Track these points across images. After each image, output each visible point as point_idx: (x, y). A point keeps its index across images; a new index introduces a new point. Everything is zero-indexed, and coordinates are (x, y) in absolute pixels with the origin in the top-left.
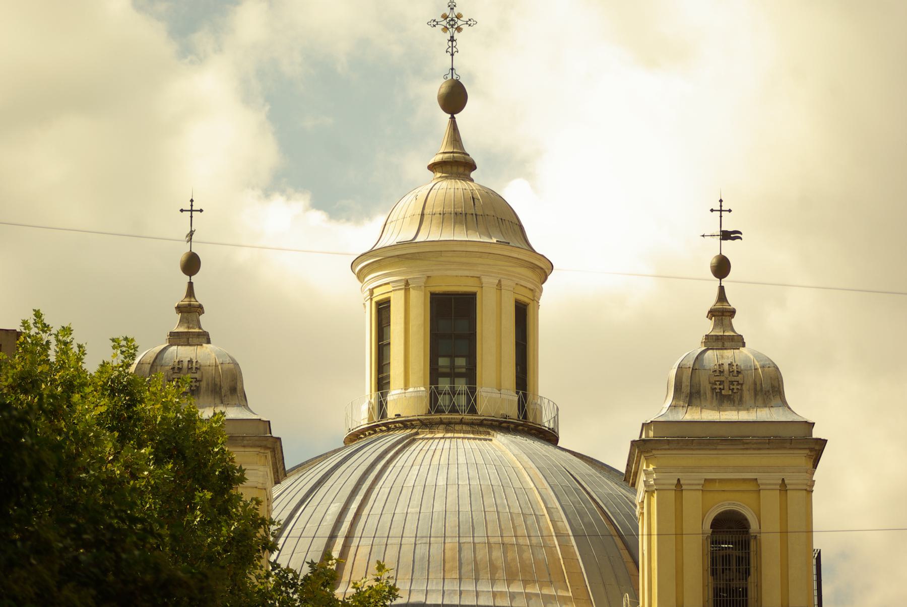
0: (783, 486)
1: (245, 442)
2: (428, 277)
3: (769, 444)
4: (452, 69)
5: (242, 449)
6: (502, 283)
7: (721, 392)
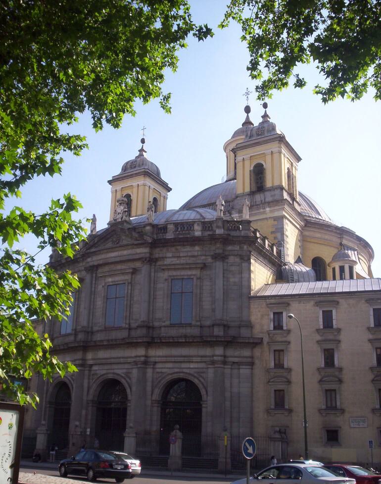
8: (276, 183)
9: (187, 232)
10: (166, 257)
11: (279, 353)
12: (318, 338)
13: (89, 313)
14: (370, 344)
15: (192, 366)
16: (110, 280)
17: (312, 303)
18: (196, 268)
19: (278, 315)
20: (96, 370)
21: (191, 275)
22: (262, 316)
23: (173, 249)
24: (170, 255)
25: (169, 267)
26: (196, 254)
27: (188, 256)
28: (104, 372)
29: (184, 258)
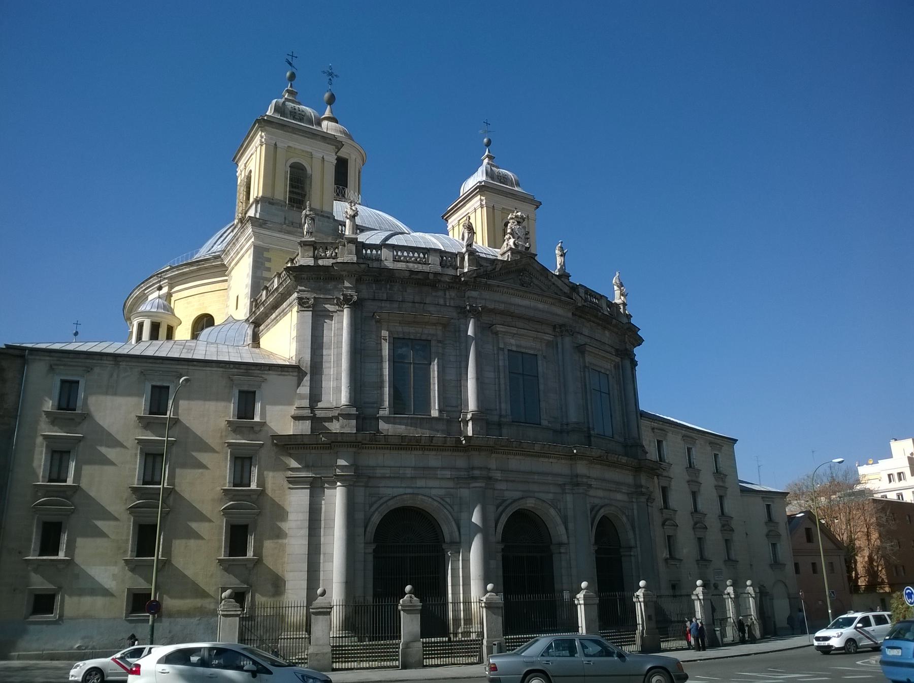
5: (327, 145)
10: (582, 334)
11: (665, 491)
12: (688, 478)
14: (715, 490)
15: (619, 497)
16: (513, 341)
17: (680, 437)
19: (660, 443)
20: (504, 490)
22: (650, 442)
28: (518, 495)
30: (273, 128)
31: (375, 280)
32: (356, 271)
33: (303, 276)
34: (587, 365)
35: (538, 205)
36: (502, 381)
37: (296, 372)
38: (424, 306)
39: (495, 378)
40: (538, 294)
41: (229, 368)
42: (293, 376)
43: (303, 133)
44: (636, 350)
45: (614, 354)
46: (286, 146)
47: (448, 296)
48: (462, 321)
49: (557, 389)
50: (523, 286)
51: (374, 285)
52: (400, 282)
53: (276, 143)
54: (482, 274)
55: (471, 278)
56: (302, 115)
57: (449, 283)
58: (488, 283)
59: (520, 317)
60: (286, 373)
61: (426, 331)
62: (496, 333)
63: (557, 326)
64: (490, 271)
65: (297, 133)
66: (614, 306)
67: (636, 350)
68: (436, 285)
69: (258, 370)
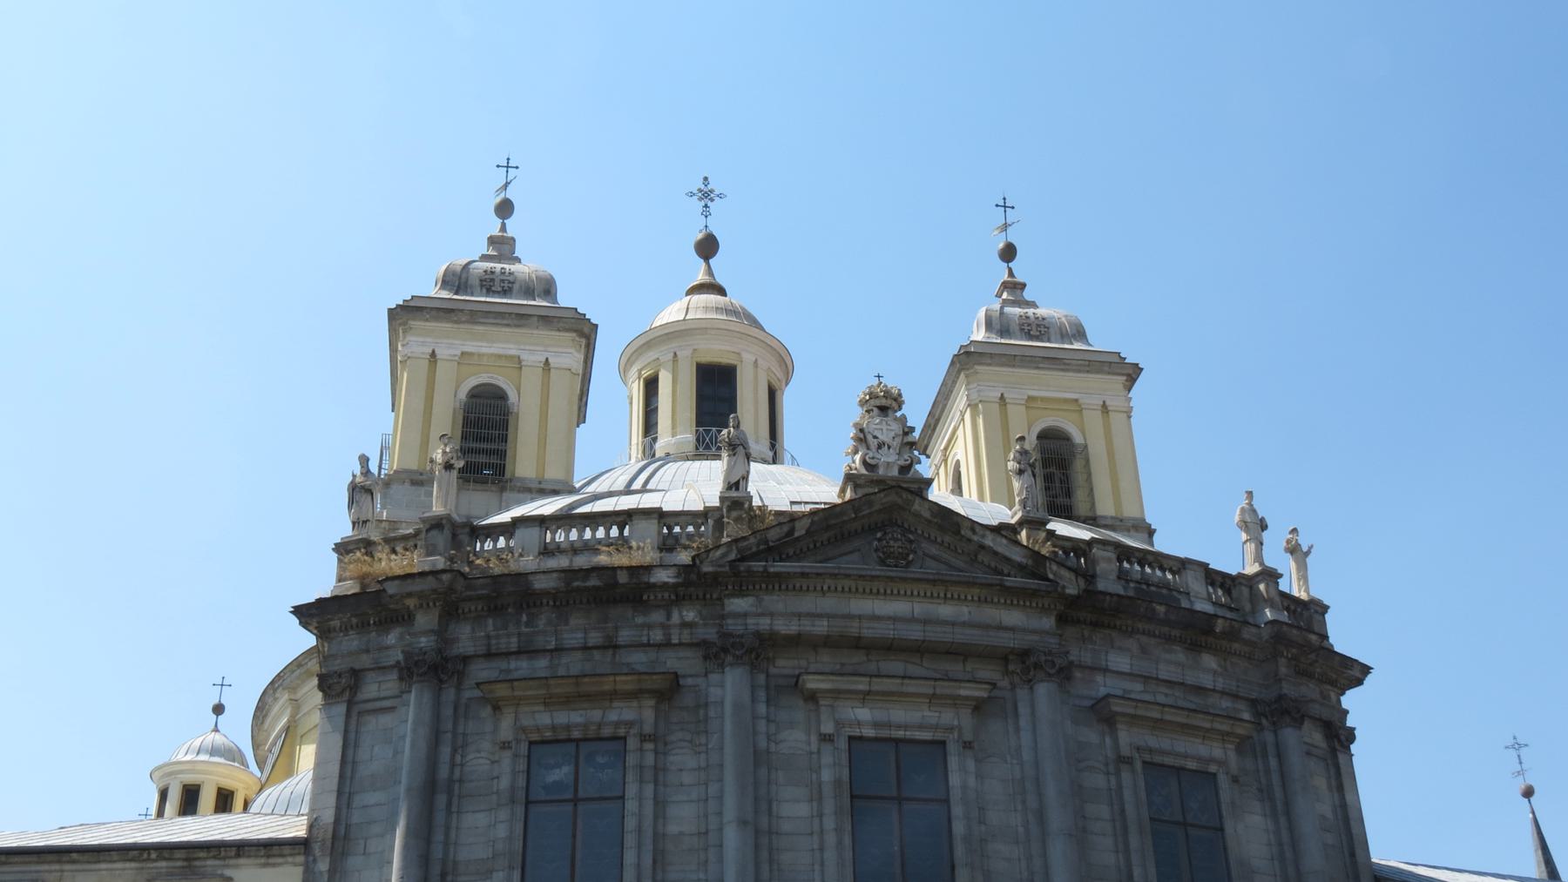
0: (1105, 408)
1: (561, 324)
2: (695, 350)
3: (1089, 366)
4: (706, 226)
5: (558, 333)
6: (759, 362)
7: (1029, 333)
8: (1129, 512)
9: (1164, 591)
10: (1106, 671)
13: (757, 847)
16: (864, 714)
18: (1224, 736)
21: (1211, 760)
23: (1131, 643)
24: (1120, 661)
25: (1140, 712)
26: (1207, 681)
27: (1182, 684)
29: (1167, 691)
30: (427, 320)
31: (489, 607)
32: (435, 591)
33: (332, 623)
34: (1125, 751)
35: (1132, 373)
36: (829, 823)
37: (299, 854)
38: (614, 655)
39: (812, 817)
40: (928, 581)
41: (149, 859)
42: (295, 865)
43: (495, 318)
44: (1349, 700)
45: (1246, 716)
46: (459, 353)
47: (675, 618)
48: (714, 677)
49: (1021, 829)
50: (882, 562)
51: (490, 621)
52: (551, 603)
53: (433, 351)
54: (754, 549)
55: (720, 566)
56: (510, 282)
57: (675, 586)
58: (772, 570)
59: (890, 648)
60: (280, 860)
61: (613, 716)
62: (812, 697)
63: (1011, 657)
64: (779, 540)
65: (482, 320)
66: (1240, 584)
67: (1349, 700)
68: (642, 597)
69: (215, 857)
